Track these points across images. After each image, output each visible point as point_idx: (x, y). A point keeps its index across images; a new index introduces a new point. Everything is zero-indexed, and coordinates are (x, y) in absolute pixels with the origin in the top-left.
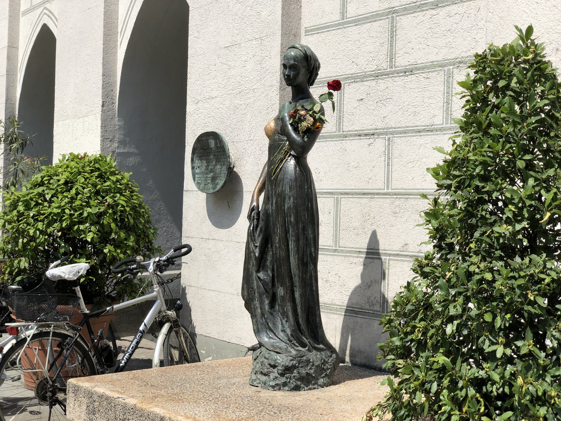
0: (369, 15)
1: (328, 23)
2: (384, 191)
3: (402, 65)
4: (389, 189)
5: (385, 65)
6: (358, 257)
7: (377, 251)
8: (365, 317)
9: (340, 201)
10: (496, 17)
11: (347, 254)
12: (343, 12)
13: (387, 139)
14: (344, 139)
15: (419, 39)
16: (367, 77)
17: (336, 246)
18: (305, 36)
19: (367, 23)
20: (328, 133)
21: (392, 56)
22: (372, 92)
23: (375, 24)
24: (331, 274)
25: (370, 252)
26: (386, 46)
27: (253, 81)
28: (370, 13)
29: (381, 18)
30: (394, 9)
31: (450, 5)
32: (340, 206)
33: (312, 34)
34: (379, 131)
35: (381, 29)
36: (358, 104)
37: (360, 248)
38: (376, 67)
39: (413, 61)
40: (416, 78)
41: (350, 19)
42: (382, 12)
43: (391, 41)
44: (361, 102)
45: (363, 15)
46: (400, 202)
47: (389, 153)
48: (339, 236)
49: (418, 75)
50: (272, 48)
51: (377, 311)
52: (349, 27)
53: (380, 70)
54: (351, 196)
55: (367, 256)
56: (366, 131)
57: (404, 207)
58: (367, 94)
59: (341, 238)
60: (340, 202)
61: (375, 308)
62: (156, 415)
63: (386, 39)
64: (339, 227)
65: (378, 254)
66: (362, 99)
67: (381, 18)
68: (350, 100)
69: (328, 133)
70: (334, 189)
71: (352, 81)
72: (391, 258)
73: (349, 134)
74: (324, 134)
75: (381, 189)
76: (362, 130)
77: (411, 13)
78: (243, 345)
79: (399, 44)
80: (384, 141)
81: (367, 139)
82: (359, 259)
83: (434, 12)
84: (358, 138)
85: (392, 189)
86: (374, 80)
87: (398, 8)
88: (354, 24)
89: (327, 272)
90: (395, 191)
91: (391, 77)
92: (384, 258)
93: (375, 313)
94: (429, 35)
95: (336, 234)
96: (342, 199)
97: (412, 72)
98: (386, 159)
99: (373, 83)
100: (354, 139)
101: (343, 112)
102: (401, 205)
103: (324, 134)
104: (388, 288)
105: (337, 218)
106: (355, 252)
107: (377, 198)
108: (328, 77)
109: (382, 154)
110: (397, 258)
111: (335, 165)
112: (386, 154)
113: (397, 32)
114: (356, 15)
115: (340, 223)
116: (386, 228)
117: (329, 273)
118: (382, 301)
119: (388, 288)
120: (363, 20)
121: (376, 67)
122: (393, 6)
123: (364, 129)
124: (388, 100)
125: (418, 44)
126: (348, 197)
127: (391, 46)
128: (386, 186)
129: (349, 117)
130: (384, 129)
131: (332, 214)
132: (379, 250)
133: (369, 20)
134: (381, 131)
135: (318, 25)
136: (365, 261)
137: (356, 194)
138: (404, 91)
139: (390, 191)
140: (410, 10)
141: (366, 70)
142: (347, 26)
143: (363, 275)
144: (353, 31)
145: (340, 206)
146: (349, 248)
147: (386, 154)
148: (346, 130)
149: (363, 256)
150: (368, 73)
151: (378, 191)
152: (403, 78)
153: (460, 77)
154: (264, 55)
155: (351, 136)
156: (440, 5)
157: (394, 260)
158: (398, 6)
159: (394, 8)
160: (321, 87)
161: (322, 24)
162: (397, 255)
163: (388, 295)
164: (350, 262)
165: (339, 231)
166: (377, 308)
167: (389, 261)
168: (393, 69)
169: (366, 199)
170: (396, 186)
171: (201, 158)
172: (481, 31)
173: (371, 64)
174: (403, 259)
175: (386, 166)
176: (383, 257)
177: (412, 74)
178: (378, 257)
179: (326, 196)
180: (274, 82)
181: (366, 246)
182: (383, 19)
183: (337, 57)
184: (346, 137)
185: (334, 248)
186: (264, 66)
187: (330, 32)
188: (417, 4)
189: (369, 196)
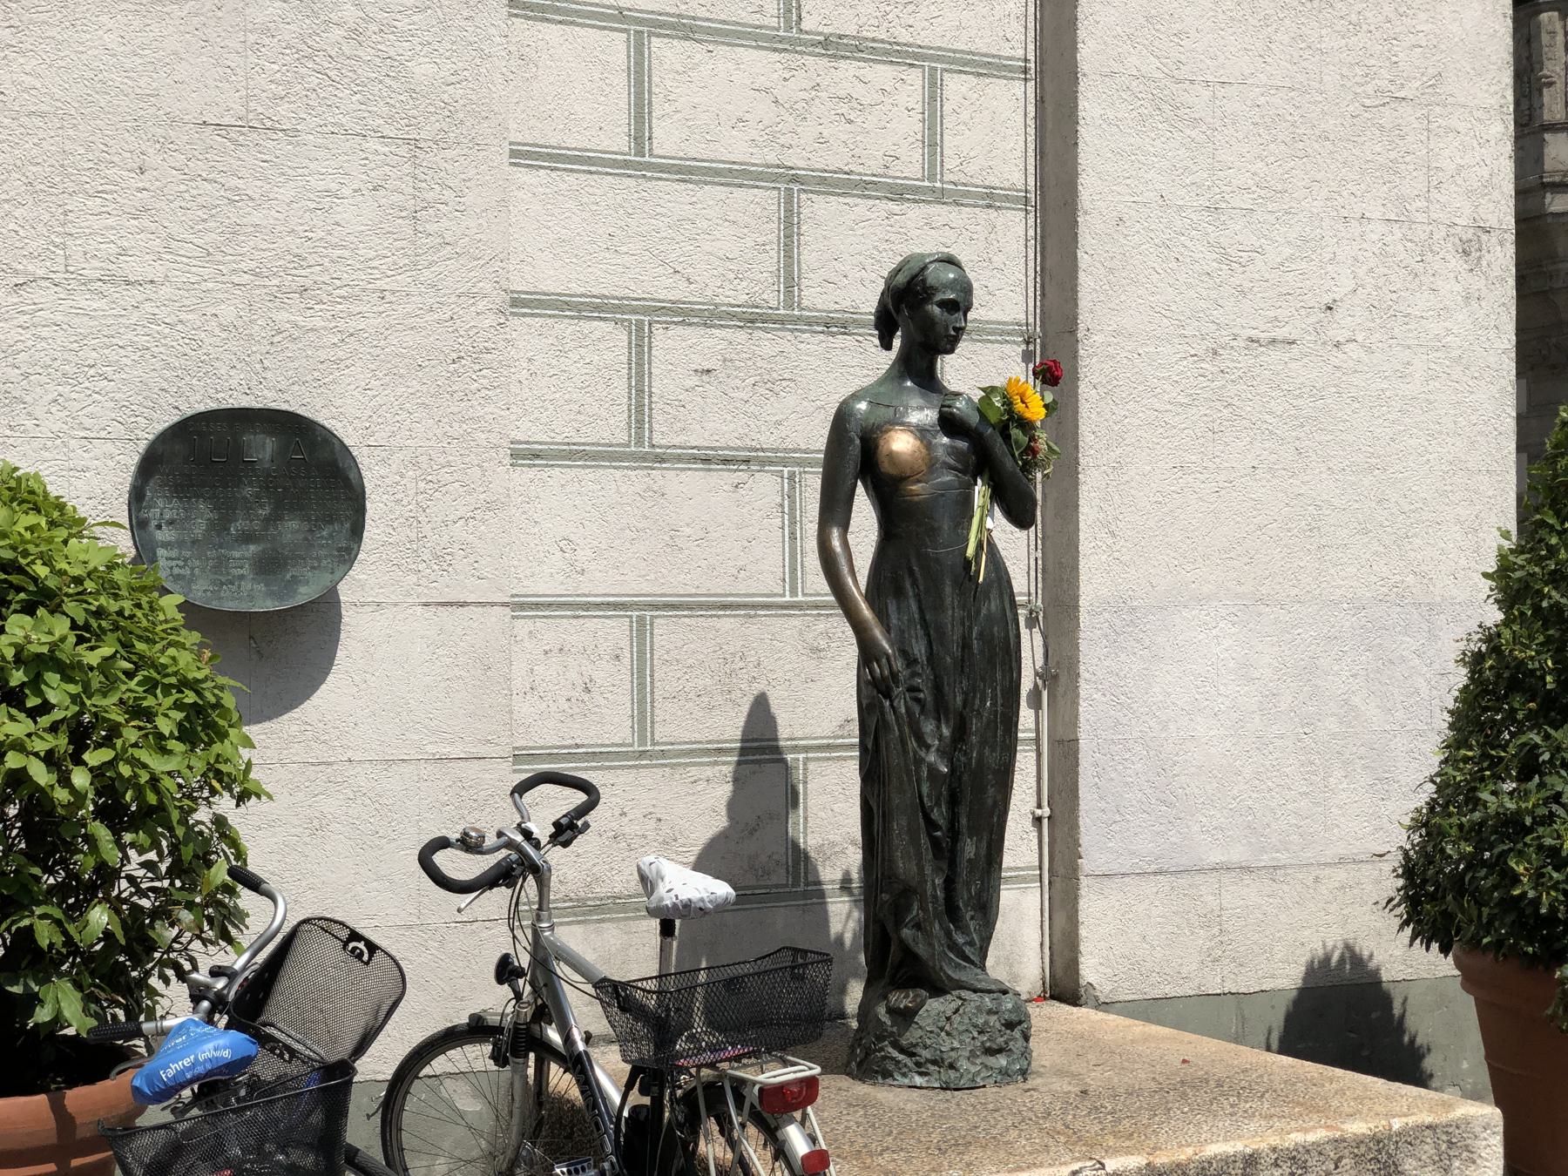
0: (722, 166)
1: (588, 150)
2: (784, 599)
3: (819, 307)
4: (797, 596)
5: (772, 298)
6: (715, 763)
7: (775, 743)
8: (747, 906)
9: (652, 624)
10: (1099, 266)
11: (682, 761)
12: (640, 135)
13: (786, 476)
14: (657, 465)
15: (861, 258)
16: (721, 318)
17: (642, 741)
20: (599, 445)
21: (790, 281)
22: (737, 357)
23: (738, 192)
24: (630, 817)
25: (751, 748)
26: (774, 253)
27: (375, 263)
29: (757, 183)
30: (794, 172)
31: (930, 202)
32: (652, 638)
33: (531, 166)
34: (763, 454)
35: (758, 210)
36: (695, 380)
37: (718, 742)
38: (747, 297)
39: (848, 304)
40: (856, 343)
41: (663, 161)
42: (761, 169)
43: (786, 245)
44: (705, 378)
46: (828, 625)
47: (792, 509)
48: (652, 715)
49: (860, 338)
50: (468, 184)
51: (777, 886)
52: (660, 179)
53: (757, 307)
54: (685, 613)
55: (743, 758)
56: (726, 452)
57: (840, 635)
58: (725, 360)
59: (657, 719)
60: (652, 629)
61: (774, 880)
62: (1228, 1161)
63: (773, 237)
64: (652, 693)
65: (777, 750)
66: (708, 371)
67: (757, 183)
68: (670, 367)
69: (599, 445)
70: (628, 595)
71: (675, 319)
72: (810, 755)
73: (671, 454)
74: (587, 448)
75: (775, 595)
76: (712, 449)
77: (839, 195)
78: (368, 1078)
79: (808, 256)
80: (779, 480)
81: (729, 470)
82: (717, 768)
83: (892, 206)
84: (701, 466)
85: (804, 595)
87: (804, 173)
88: (677, 177)
89: (617, 812)
90: (814, 599)
91: (789, 330)
92: (792, 759)
93: (774, 890)
94: (884, 254)
95: (642, 713)
96: (657, 621)
97: (845, 328)
98: (786, 522)
99: (741, 336)
100: (690, 469)
101: (650, 396)
102: (833, 630)
103: (587, 448)
104: (805, 828)
105: (641, 671)
106: (707, 752)
107: (765, 616)
108: (594, 296)
109: (774, 510)
110: (828, 755)
111: (628, 531)
112: (786, 510)
113: (804, 228)
114: (681, 154)
115: (652, 683)
116: (792, 687)
117: (623, 814)
118: (790, 861)
119: (805, 828)
120: (704, 175)
122: (792, 165)
123: (718, 444)
124: (784, 384)
125: (858, 269)
126: (676, 616)
127: (789, 256)
128: (787, 588)
129: (667, 409)
130: (776, 450)
131: (627, 661)
132: (776, 739)
133: (723, 180)
134: (770, 454)
135: (554, 148)
136: (735, 772)
137: (701, 606)
138: (828, 369)
139: (800, 598)
140: (837, 186)
141: (717, 300)
142: (655, 175)
143: (732, 806)
144: (673, 196)
145: (652, 638)
146: (686, 743)
147: (786, 510)
148: (663, 442)
149: (853, 754)
151: (765, 599)
152: (822, 337)
153: (959, 360)
154: (430, 196)
155: (679, 458)
156: (908, 196)
157: (818, 759)
158: (804, 169)
159: (793, 168)
160: (572, 317)
161: (568, 149)
162: (829, 747)
163: (805, 842)
164: (692, 779)
165: (652, 702)
166: (779, 877)
167: (805, 764)
168: (796, 313)
169: (732, 620)
170: (814, 586)
171: (184, 489)
172: (999, 276)
173: (732, 287)
174: (844, 754)
175: (787, 539)
176: (789, 757)
177: (845, 334)
178: (774, 757)
179: (601, 613)
180: (487, 286)
181: (738, 734)
182: (762, 187)
183: (624, 249)
184: (663, 461)
185: (636, 748)
186: (431, 228)
187: (595, 177)
188: (852, 177)
189: (742, 612)
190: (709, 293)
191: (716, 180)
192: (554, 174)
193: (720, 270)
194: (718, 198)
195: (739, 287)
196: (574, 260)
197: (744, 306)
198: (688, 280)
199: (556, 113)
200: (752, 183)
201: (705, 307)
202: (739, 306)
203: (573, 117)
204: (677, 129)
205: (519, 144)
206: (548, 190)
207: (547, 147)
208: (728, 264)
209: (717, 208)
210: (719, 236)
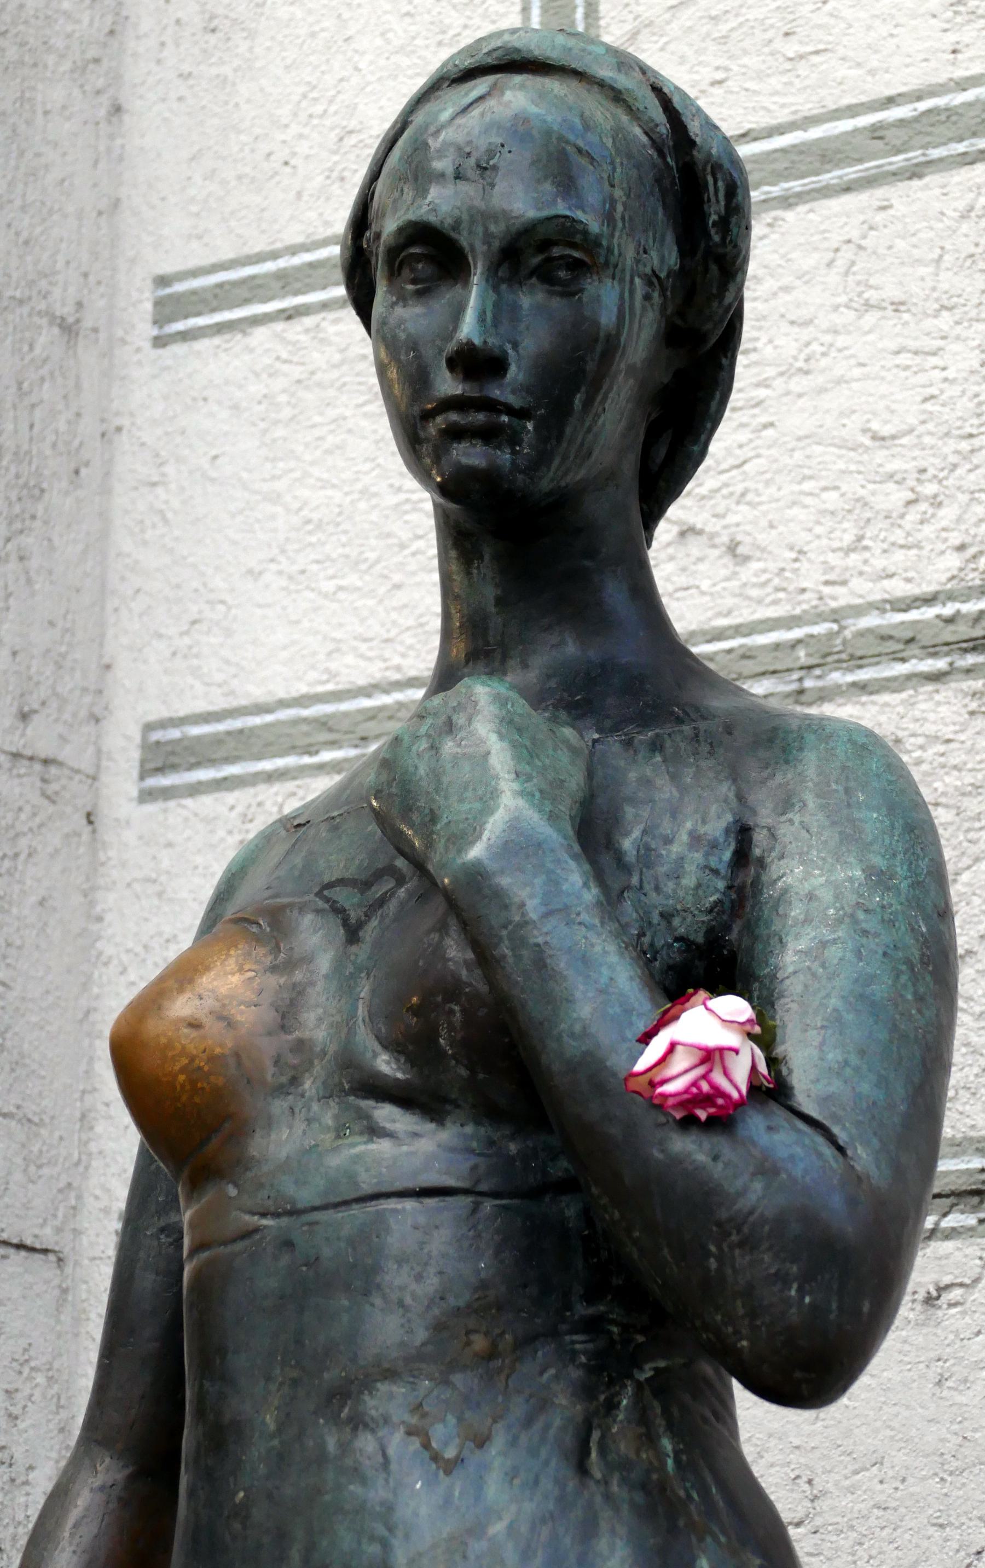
0: (846, 125)
16: (858, 661)
18: (160, 342)
19: (827, 192)
28: (852, 111)
45: (779, 130)
86: (936, 677)
121: (953, 561)
133: (851, 172)
135: (293, 250)
141: (842, 597)
150: (871, 621)
173: (898, 536)
190: (811, 577)
191: (826, 178)
192: (295, 330)
193: (852, 486)
194: (835, 239)
195: (928, 530)
196: (352, 579)
197: (951, 597)
198: (732, 548)
199: (303, 148)
200: (961, 148)
201: (797, 633)
202: (929, 600)
203: (353, 140)
204: (683, 60)
205: (195, 273)
206: (279, 384)
207: (274, 255)
208: (880, 456)
209: (833, 277)
210: (838, 371)
